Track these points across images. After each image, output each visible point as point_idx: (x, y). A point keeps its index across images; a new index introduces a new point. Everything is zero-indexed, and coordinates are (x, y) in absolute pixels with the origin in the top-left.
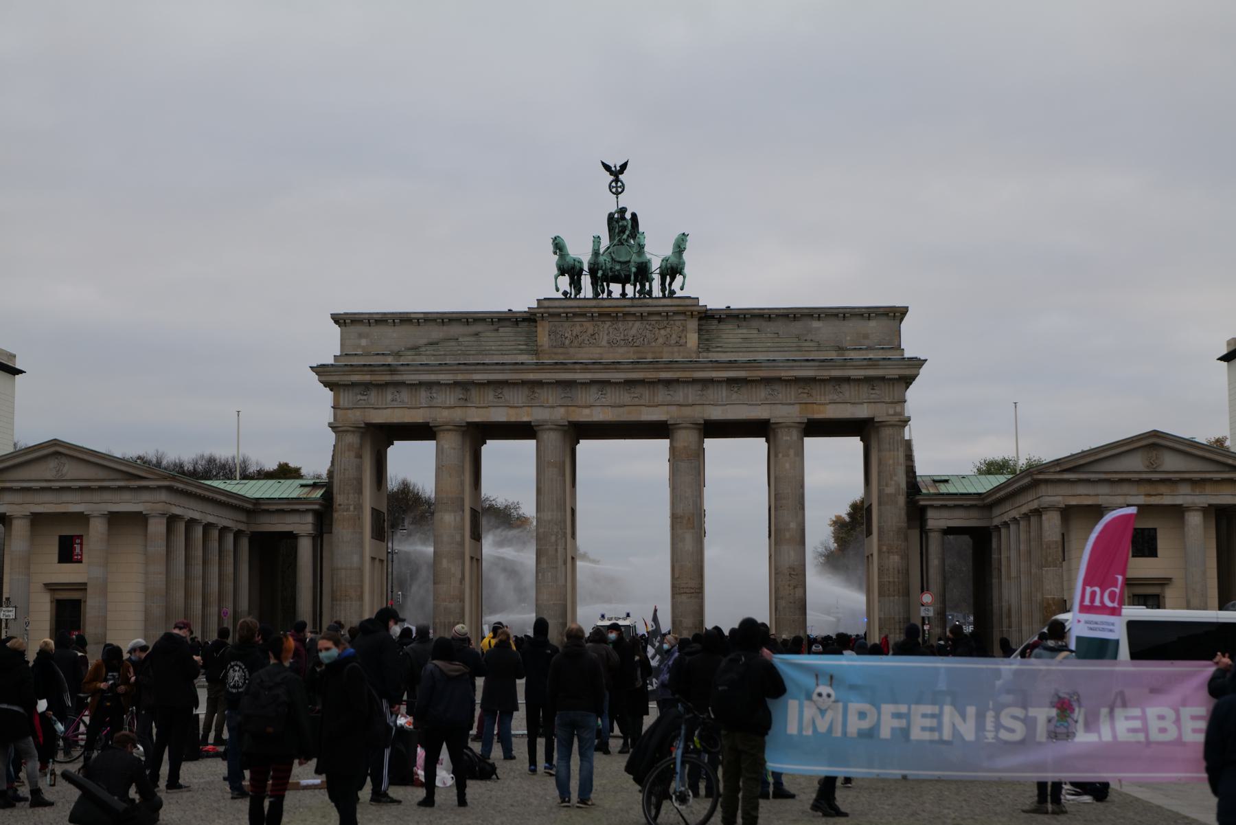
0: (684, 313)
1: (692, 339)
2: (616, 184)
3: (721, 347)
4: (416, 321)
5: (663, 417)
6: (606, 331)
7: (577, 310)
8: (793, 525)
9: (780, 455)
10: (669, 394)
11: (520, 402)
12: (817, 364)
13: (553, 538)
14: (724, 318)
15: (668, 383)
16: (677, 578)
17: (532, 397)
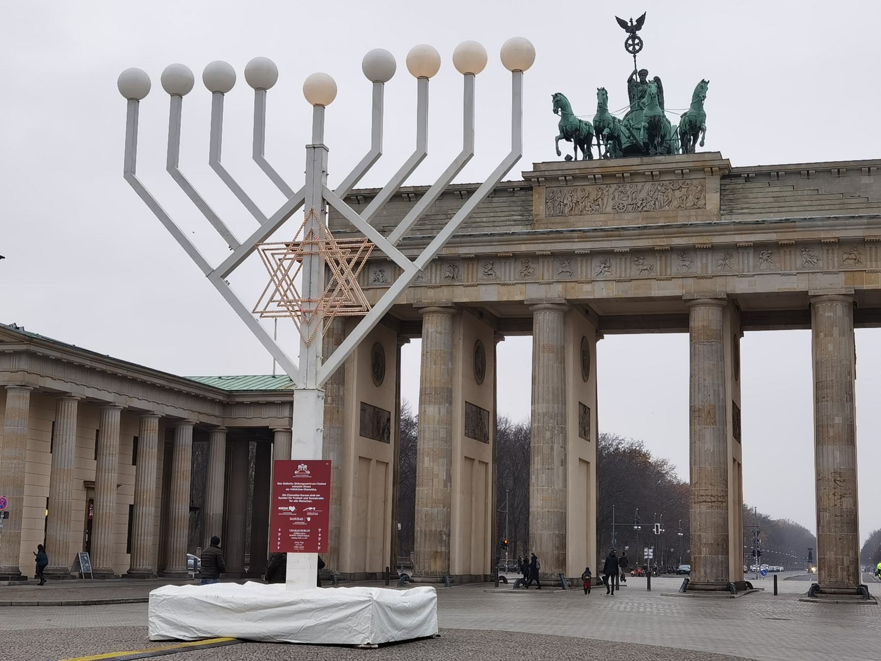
0: (702, 170)
1: (713, 200)
2: (633, 41)
3: (748, 208)
4: (406, 195)
5: (678, 293)
6: (611, 195)
7: (577, 172)
8: (838, 420)
9: (822, 335)
10: (683, 266)
11: (512, 279)
12: (865, 221)
13: (548, 434)
14: (752, 177)
15: (684, 251)
16: (697, 483)
17: (527, 273)
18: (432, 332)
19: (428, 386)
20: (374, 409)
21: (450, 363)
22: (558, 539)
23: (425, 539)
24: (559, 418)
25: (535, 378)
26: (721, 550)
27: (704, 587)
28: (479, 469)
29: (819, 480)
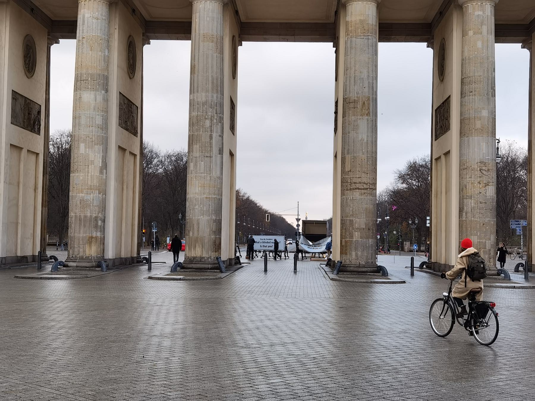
8: (485, 113)
9: (471, 33)
13: (208, 123)
16: (350, 171)
18: (88, 18)
19: (84, 71)
20: (25, 99)
21: (106, 51)
22: (215, 224)
23: (80, 224)
24: (218, 108)
25: (194, 67)
26: (371, 234)
27: (356, 269)
28: (128, 158)
29: (464, 169)
